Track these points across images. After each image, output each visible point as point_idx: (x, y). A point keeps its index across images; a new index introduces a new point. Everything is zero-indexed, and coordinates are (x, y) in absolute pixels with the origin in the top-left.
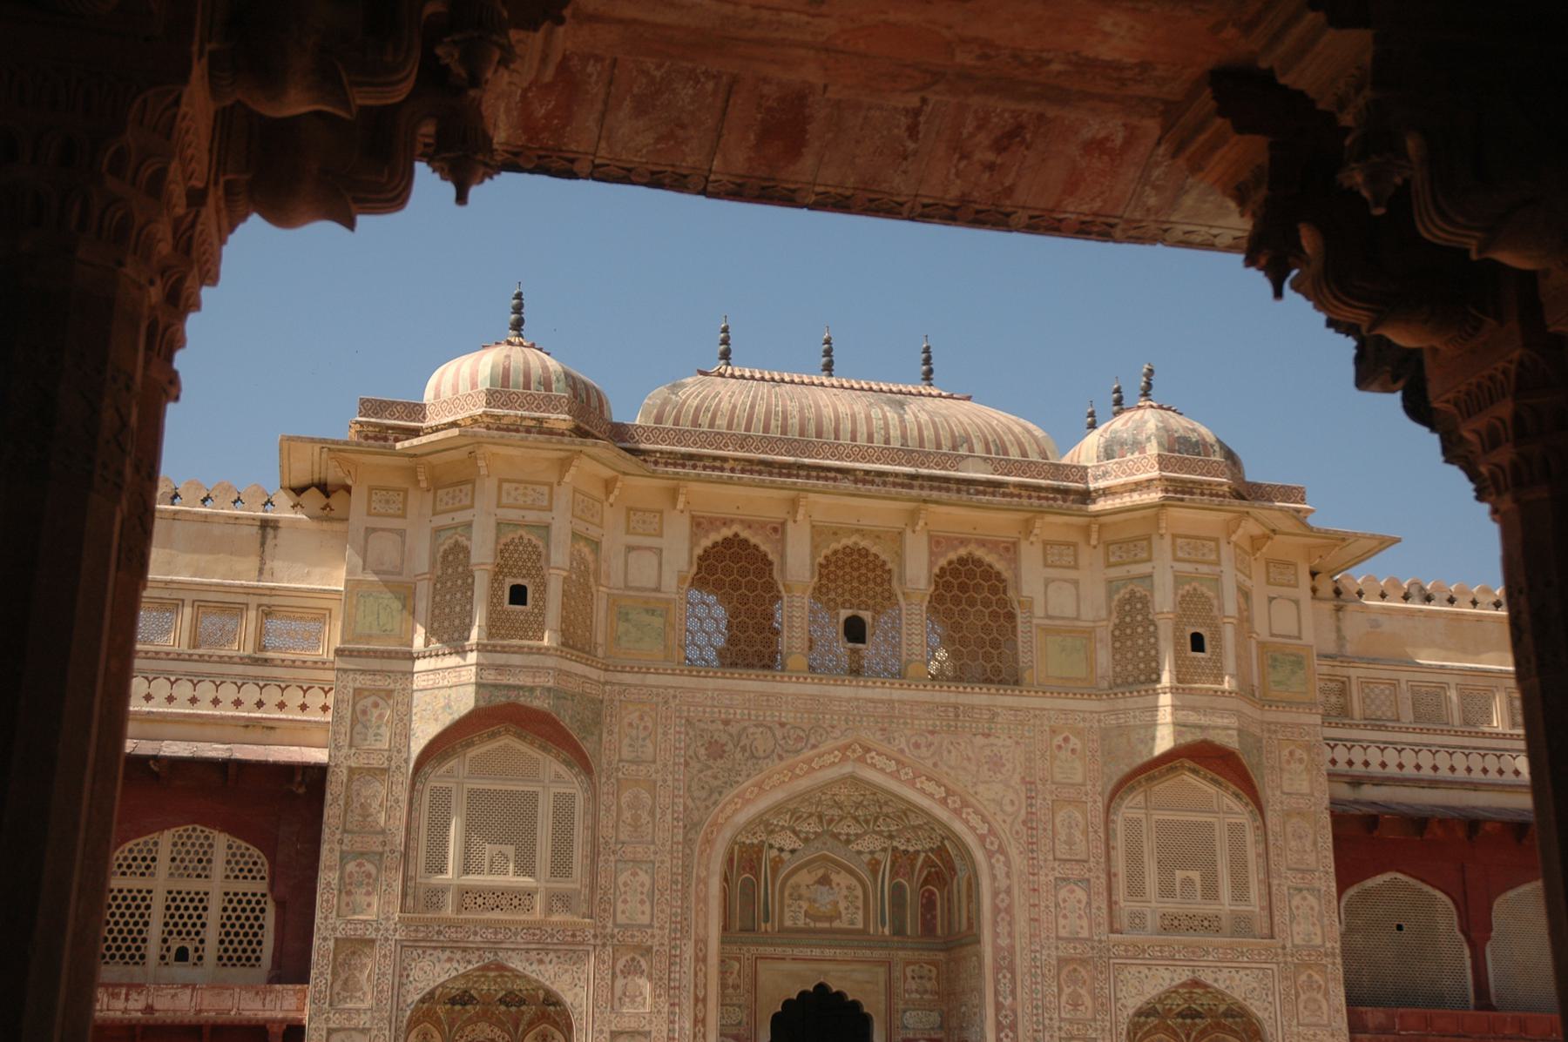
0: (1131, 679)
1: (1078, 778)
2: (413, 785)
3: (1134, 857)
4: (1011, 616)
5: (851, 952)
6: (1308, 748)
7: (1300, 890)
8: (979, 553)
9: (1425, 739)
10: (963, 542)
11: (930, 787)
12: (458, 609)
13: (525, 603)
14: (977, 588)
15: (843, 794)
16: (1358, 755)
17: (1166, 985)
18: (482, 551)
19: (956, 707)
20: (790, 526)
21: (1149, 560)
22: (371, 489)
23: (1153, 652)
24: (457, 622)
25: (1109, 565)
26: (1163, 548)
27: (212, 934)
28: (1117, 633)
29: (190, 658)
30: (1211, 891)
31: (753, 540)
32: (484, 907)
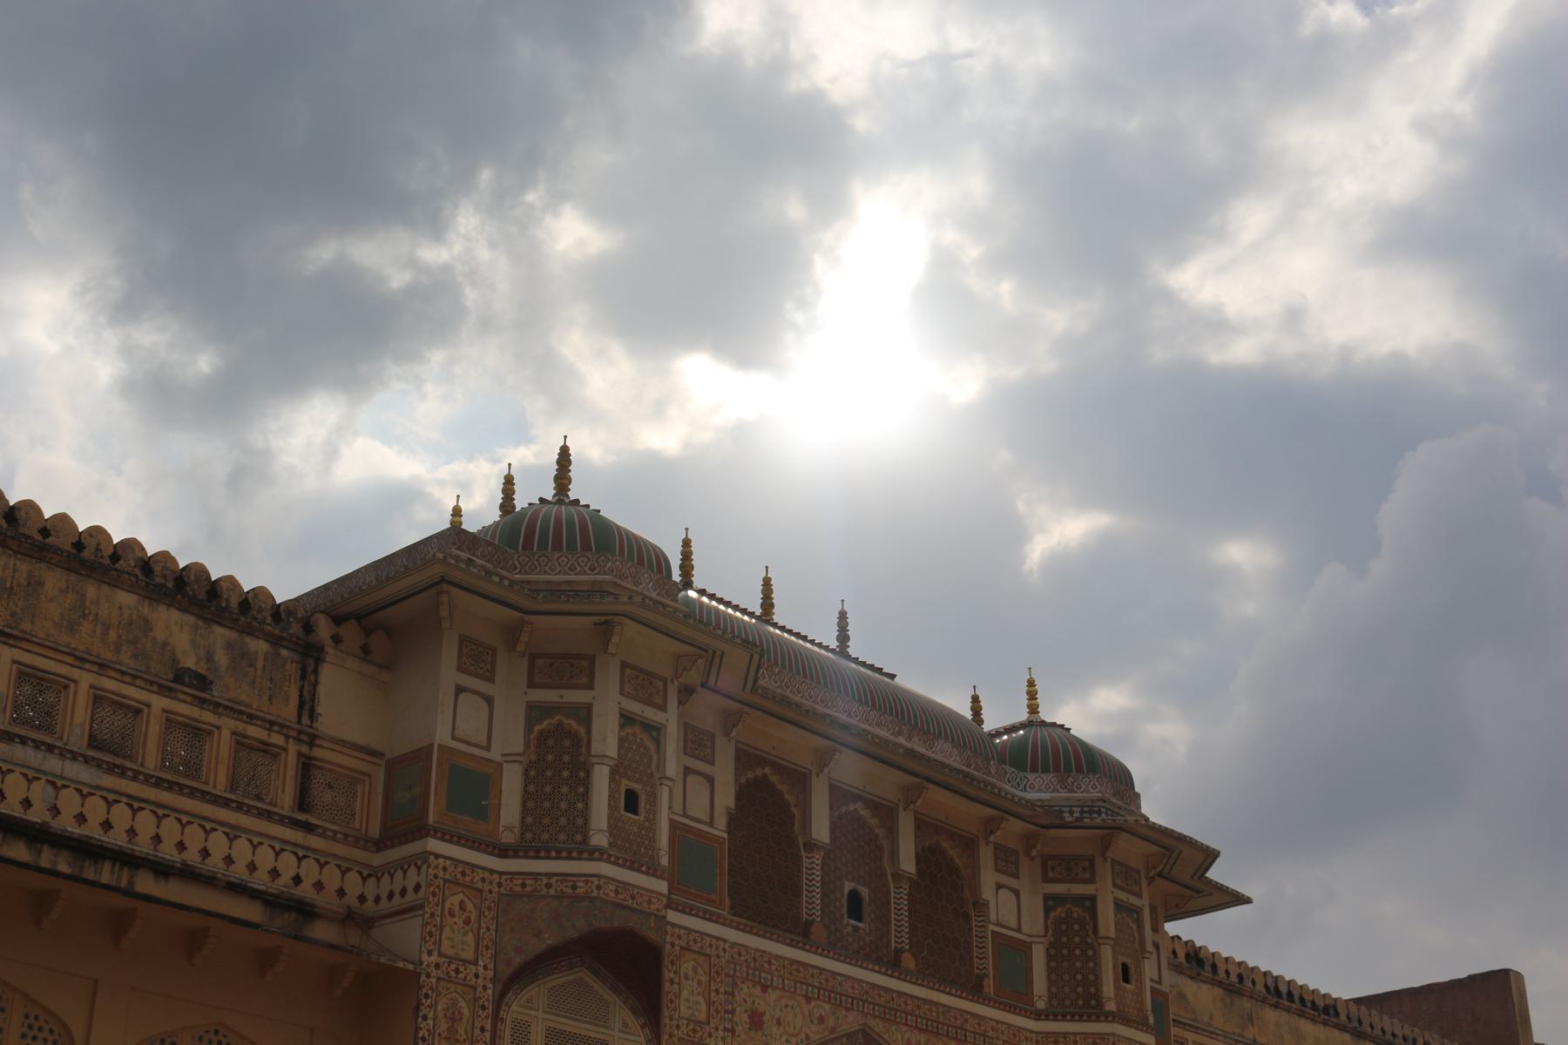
0: (1068, 1002)
4: (967, 917)
8: (944, 844)
12: (564, 805)
13: (635, 812)
19: (937, 1004)
21: (1092, 880)
22: (464, 641)
23: (1092, 977)
24: (563, 821)
25: (1046, 880)
26: (1105, 871)
28: (1052, 952)
29: (225, 803)
31: (780, 787)
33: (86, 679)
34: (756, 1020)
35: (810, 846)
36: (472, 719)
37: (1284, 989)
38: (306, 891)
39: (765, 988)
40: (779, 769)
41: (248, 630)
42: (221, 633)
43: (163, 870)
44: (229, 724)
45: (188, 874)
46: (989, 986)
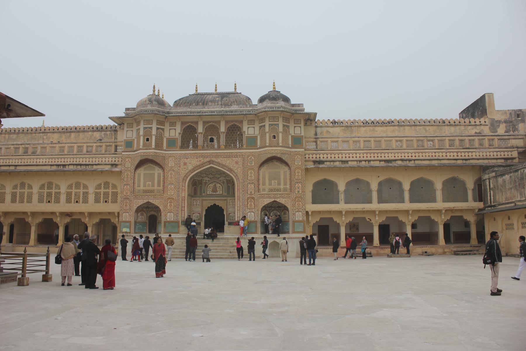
1: (253, 165)
2: (134, 173)
3: (264, 178)
4: (242, 135)
5: (219, 198)
6: (302, 155)
7: (297, 183)
8: (236, 123)
9: (333, 152)
10: (232, 121)
11: (225, 168)
14: (236, 130)
15: (213, 170)
16: (318, 156)
17: (269, 202)
18: (142, 133)
20: (199, 123)
27: (110, 198)
30: (279, 184)
32: (146, 193)
33: (85, 145)
34: (185, 164)
35: (199, 133)
36: (129, 134)
37: (370, 122)
38: (116, 163)
39: (187, 159)
40: (192, 122)
41: (106, 131)
42: (103, 133)
43: (96, 165)
44: (104, 144)
45: (98, 164)
46: (245, 146)
